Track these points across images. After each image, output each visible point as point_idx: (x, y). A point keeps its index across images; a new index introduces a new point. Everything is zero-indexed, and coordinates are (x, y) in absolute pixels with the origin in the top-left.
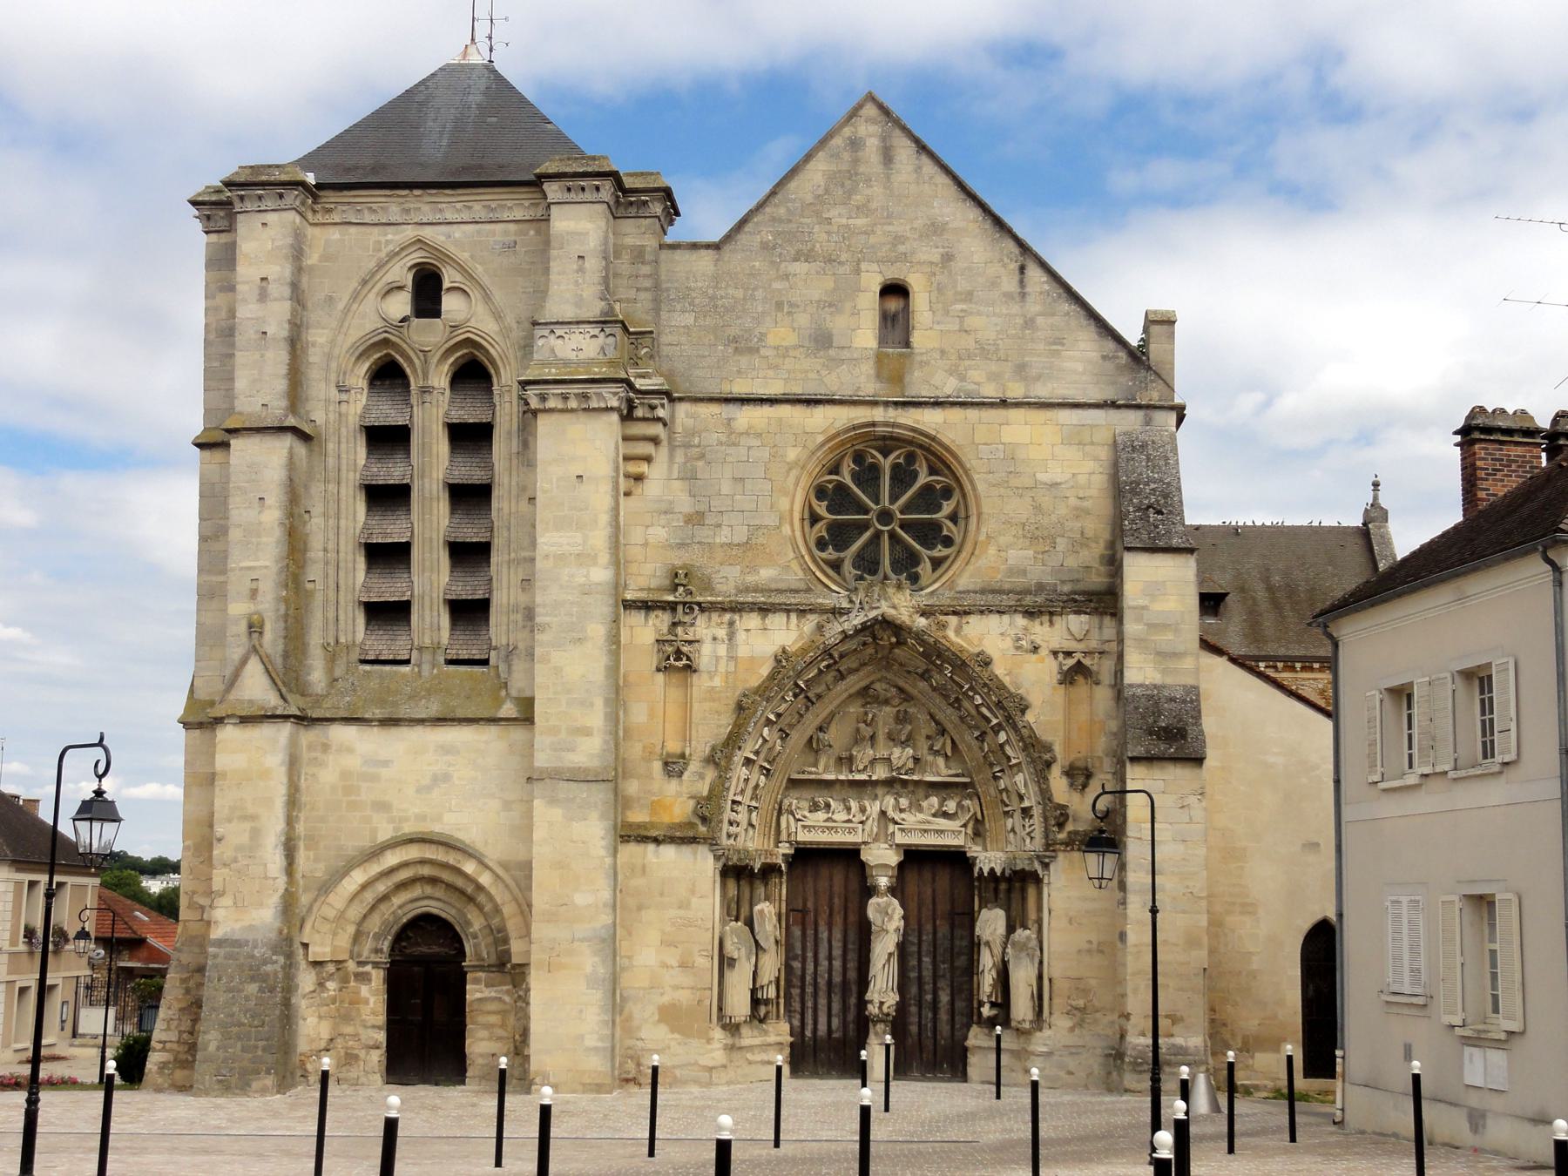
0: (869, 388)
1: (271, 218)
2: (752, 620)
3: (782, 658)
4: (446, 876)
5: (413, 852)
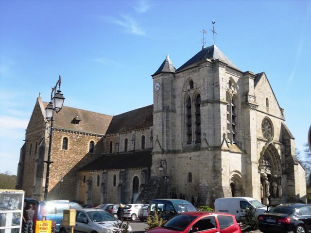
0: (266, 112)
1: (223, 68)
2: (261, 142)
3: (264, 148)
4: (236, 177)
5: (235, 173)
